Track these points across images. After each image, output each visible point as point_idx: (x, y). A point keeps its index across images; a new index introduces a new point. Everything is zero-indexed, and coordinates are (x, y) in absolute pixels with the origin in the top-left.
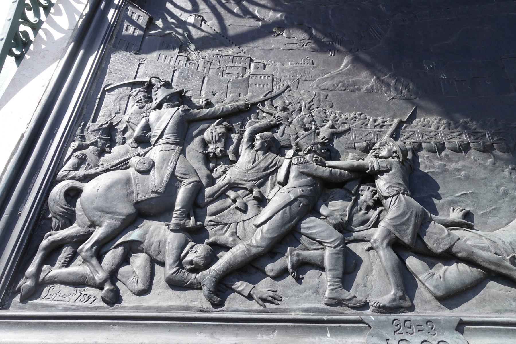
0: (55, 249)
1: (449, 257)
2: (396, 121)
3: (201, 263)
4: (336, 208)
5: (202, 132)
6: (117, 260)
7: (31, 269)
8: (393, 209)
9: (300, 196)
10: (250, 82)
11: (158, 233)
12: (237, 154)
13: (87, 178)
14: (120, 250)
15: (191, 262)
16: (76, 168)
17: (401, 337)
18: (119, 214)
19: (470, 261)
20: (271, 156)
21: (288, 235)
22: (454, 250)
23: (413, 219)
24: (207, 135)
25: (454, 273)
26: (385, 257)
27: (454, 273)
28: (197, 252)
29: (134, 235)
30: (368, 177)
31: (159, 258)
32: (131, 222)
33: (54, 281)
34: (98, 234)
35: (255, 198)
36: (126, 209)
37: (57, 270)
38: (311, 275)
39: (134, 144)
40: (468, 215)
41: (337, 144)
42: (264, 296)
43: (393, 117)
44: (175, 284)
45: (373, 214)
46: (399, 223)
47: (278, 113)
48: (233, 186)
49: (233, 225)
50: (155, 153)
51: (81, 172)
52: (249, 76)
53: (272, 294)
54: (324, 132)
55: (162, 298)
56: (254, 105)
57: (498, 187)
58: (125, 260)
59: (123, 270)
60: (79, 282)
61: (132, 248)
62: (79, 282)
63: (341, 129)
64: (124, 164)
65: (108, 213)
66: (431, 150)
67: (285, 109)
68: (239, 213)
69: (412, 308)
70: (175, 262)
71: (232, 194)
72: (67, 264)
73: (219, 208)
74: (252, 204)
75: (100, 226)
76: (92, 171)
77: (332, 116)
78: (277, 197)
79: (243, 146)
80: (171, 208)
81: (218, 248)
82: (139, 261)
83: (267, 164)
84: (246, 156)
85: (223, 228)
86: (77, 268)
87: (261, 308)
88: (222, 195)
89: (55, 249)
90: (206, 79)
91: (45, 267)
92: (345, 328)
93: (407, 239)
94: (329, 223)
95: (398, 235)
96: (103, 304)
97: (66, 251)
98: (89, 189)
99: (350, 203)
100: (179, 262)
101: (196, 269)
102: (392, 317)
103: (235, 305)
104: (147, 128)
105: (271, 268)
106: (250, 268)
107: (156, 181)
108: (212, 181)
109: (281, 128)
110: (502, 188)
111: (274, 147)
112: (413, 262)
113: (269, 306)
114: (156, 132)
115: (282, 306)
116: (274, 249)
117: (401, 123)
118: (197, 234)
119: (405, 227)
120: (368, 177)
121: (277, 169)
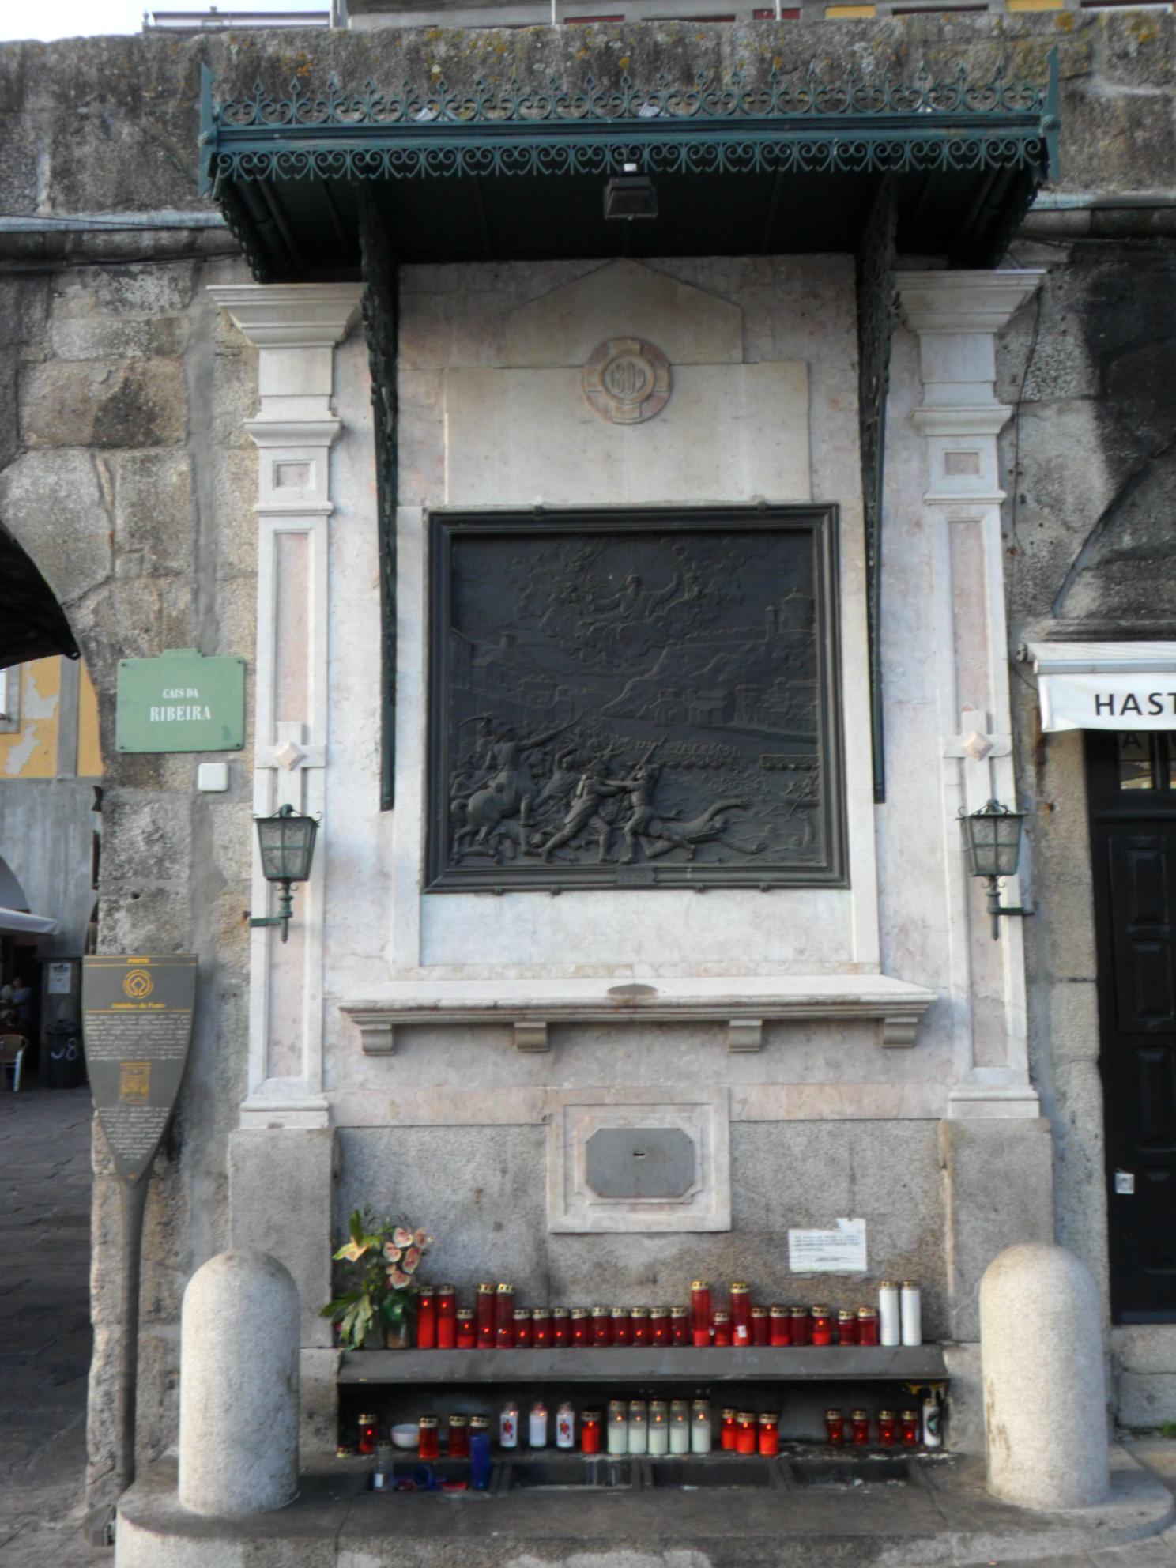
0: (462, 838)
1: (659, 837)
4: (610, 808)
5: (528, 757)
7: (455, 849)
8: (639, 812)
11: (516, 827)
12: (551, 771)
13: (469, 796)
16: (459, 789)
19: (669, 839)
20: (573, 774)
21: (582, 825)
24: (532, 760)
25: (660, 845)
26: (629, 839)
27: (660, 845)
28: (537, 838)
29: (502, 830)
30: (625, 791)
32: (498, 823)
33: (468, 854)
36: (496, 816)
38: (592, 847)
40: (679, 812)
41: (614, 765)
44: (528, 854)
46: (638, 824)
47: (577, 739)
48: (551, 797)
50: (502, 777)
54: (607, 752)
55: (524, 861)
56: (560, 732)
58: (500, 843)
59: (501, 847)
61: (503, 837)
62: (480, 854)
64: (485, 786)
66: (672, 767)
67: (581, 735)
71: (552, 802)
72: (471, 845)
78: (577, 805)
79: (555, 768)
80: (518, 811)
81: (547, 836)
82: (507, 843)
84: (557, 775)
86: (476, 848)
88: (545, 802)
97: (468, 839)
98: (472, 804)
100: (528, 843)
103: (558, 864)
104: (494, 758)
105: (574, 843)
106: (563, 844)
107: (507, 797)
108: (539, 792)
111: (575, 767)
112: (643, 840)
114: (501, 760)
116: (574, 835)
118: (533, 827)
120: (625, 791)
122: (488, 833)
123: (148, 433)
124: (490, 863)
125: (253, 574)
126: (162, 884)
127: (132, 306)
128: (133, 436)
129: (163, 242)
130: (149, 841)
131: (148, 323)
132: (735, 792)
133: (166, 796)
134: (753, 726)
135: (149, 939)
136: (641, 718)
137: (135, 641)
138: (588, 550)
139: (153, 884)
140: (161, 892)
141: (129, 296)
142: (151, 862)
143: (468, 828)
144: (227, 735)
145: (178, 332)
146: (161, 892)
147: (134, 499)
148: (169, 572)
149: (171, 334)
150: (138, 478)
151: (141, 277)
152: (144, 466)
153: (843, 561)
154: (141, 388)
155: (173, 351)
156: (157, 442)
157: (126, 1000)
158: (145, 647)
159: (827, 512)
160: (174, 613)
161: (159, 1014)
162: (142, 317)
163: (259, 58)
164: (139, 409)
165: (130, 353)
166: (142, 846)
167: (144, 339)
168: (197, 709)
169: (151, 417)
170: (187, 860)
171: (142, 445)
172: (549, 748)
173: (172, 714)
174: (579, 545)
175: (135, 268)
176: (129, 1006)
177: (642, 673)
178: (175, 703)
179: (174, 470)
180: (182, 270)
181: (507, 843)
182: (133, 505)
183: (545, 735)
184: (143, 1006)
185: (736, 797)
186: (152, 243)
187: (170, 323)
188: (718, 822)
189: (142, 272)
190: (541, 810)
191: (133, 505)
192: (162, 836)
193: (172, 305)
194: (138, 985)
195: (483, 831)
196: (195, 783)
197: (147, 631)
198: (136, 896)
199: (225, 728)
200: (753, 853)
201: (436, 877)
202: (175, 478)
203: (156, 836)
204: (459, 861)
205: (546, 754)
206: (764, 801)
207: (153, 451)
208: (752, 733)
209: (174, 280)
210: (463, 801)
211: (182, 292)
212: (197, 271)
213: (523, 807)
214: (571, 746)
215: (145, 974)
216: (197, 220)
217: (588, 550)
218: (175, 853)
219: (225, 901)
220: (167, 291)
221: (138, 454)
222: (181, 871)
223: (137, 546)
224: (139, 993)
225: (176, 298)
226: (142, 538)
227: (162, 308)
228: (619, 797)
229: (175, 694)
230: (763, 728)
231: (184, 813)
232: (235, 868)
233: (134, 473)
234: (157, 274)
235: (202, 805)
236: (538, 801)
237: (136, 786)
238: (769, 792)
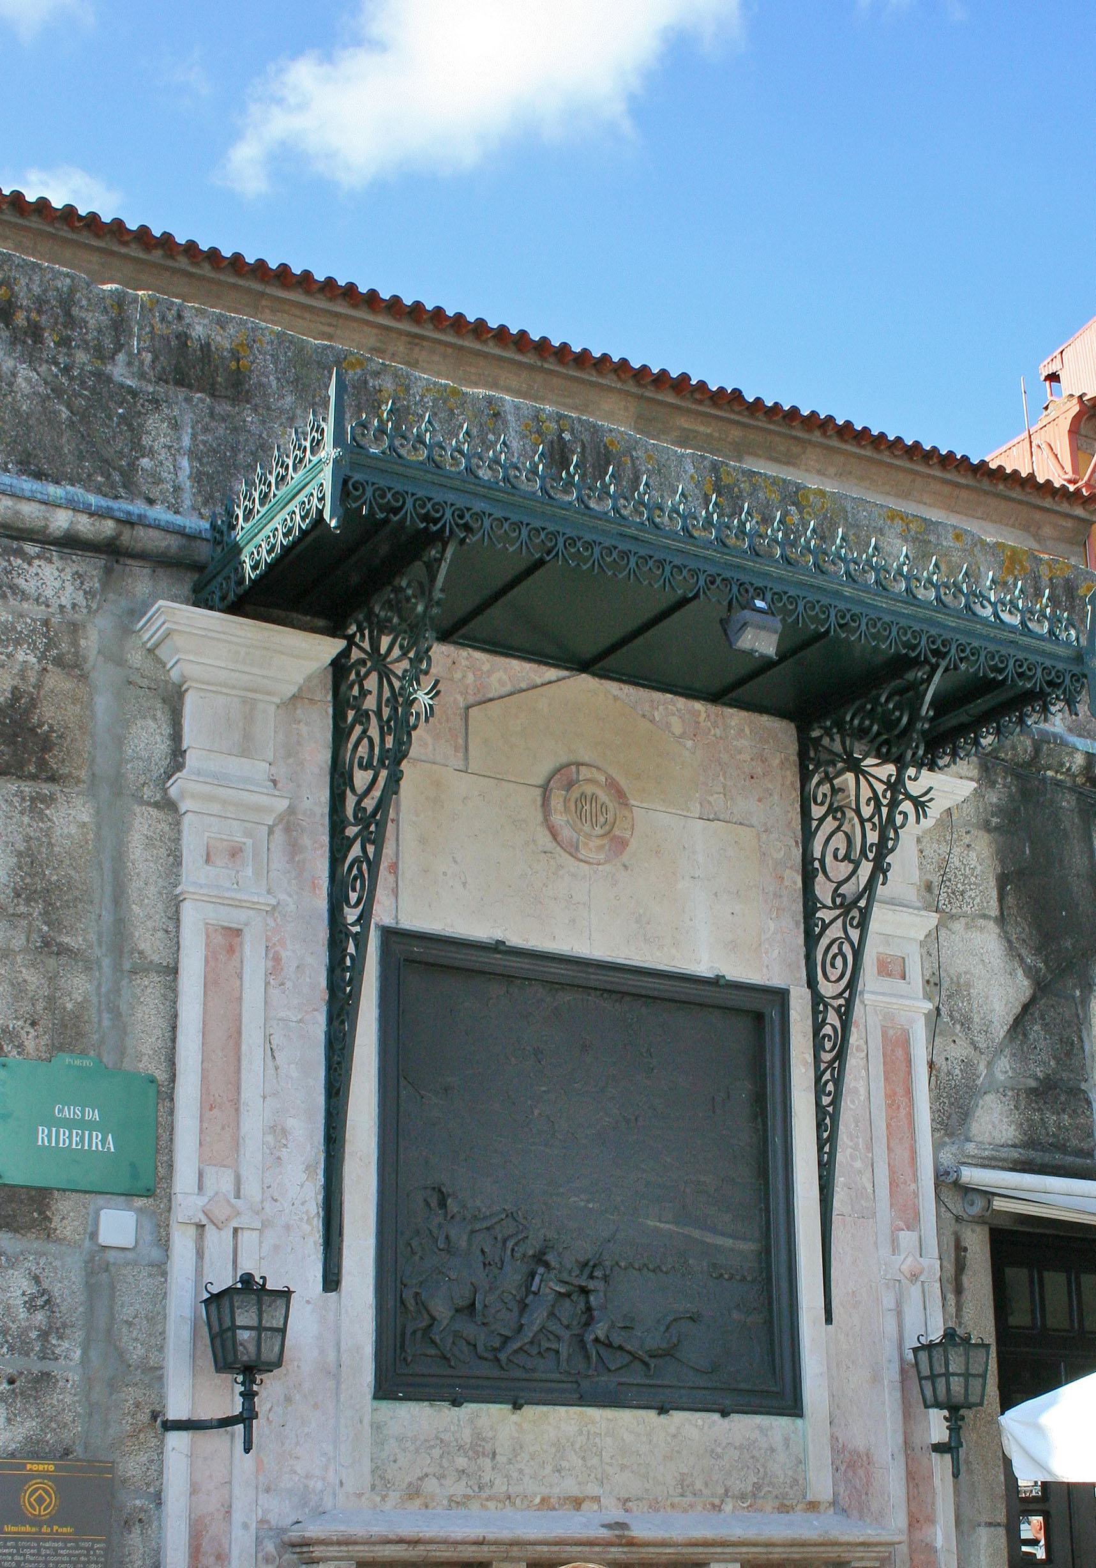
123: (42, 764)
125: (173, 971)
126: (47, 1366)
127: (25, 596)
128: (21, 765)
129: (80, 527)
130: (31, 1306)
131: (46, 623)
133: (52, 1248)
135: (28, 1439)
137: (18, 1036)
139: (37, 1367)
140: (46, 1376)
141: (29, 586)
142: (34, 1334)
144: (135, 1174)
145: (83, 642)
146: (46, 1376)
147: (22, 847)
148: (63, 951)
149: (75, 643)
150: (26, 820)
151: (37, 562)
152: (37, 805)
153: (793, 1054)
154: (33, 703)
155: (76, 666)
156: (52, 779)
157: (20, 1518)
158: (30, 1045)
159: (781, 996)
160: (69, 1006)
161: (65, 1541)
162: (39, 612)
163: (187, 336)
164: (32, 730)
165: (21, 656)
166: (22, 1314)
167: (41, 642)
168: (97, 1137)
169: (46, 745)
170: (79, 1335)
171: (34, 777)
173: (65, 1138)
175: (31, 549)
176: (28, 1528)
178: (70, 1124)
179: (72, 817)
180: (92, 567)
182: (20, 854)
184: (45, 1529)
186: (65, 525)
187: (75, 629)
189: (38, 557)
191: (20, 854)
192: (47, 1302)
193: (74, 605)
194: (40, 1500)
196: (94, 1235)
197: (33, 1024)
198: (11, 1382)
199: (133, 1165)
202: (73, 830)
203: (39, 1302)
207: (46, 788)
209: (77, 575)
211: (89, 594)
212: (108, 571)
215: (49, 1485)
216: (129, 513)
218: (64, 1325)
219: (131, 1394)
220: (69, 588)
221: (27, 788)
222: (70, 1350)
223: (22, 909)
224: (42, 1511)
225: (80, 599)
226: (28, 901)
227: (62, 607)
229: (70, 1112)
231: (76, 1277)
232: (140, 1351)
233: (22, 813)
234: (58, 563)
235: (101, 1268)
237: (16, 1231)
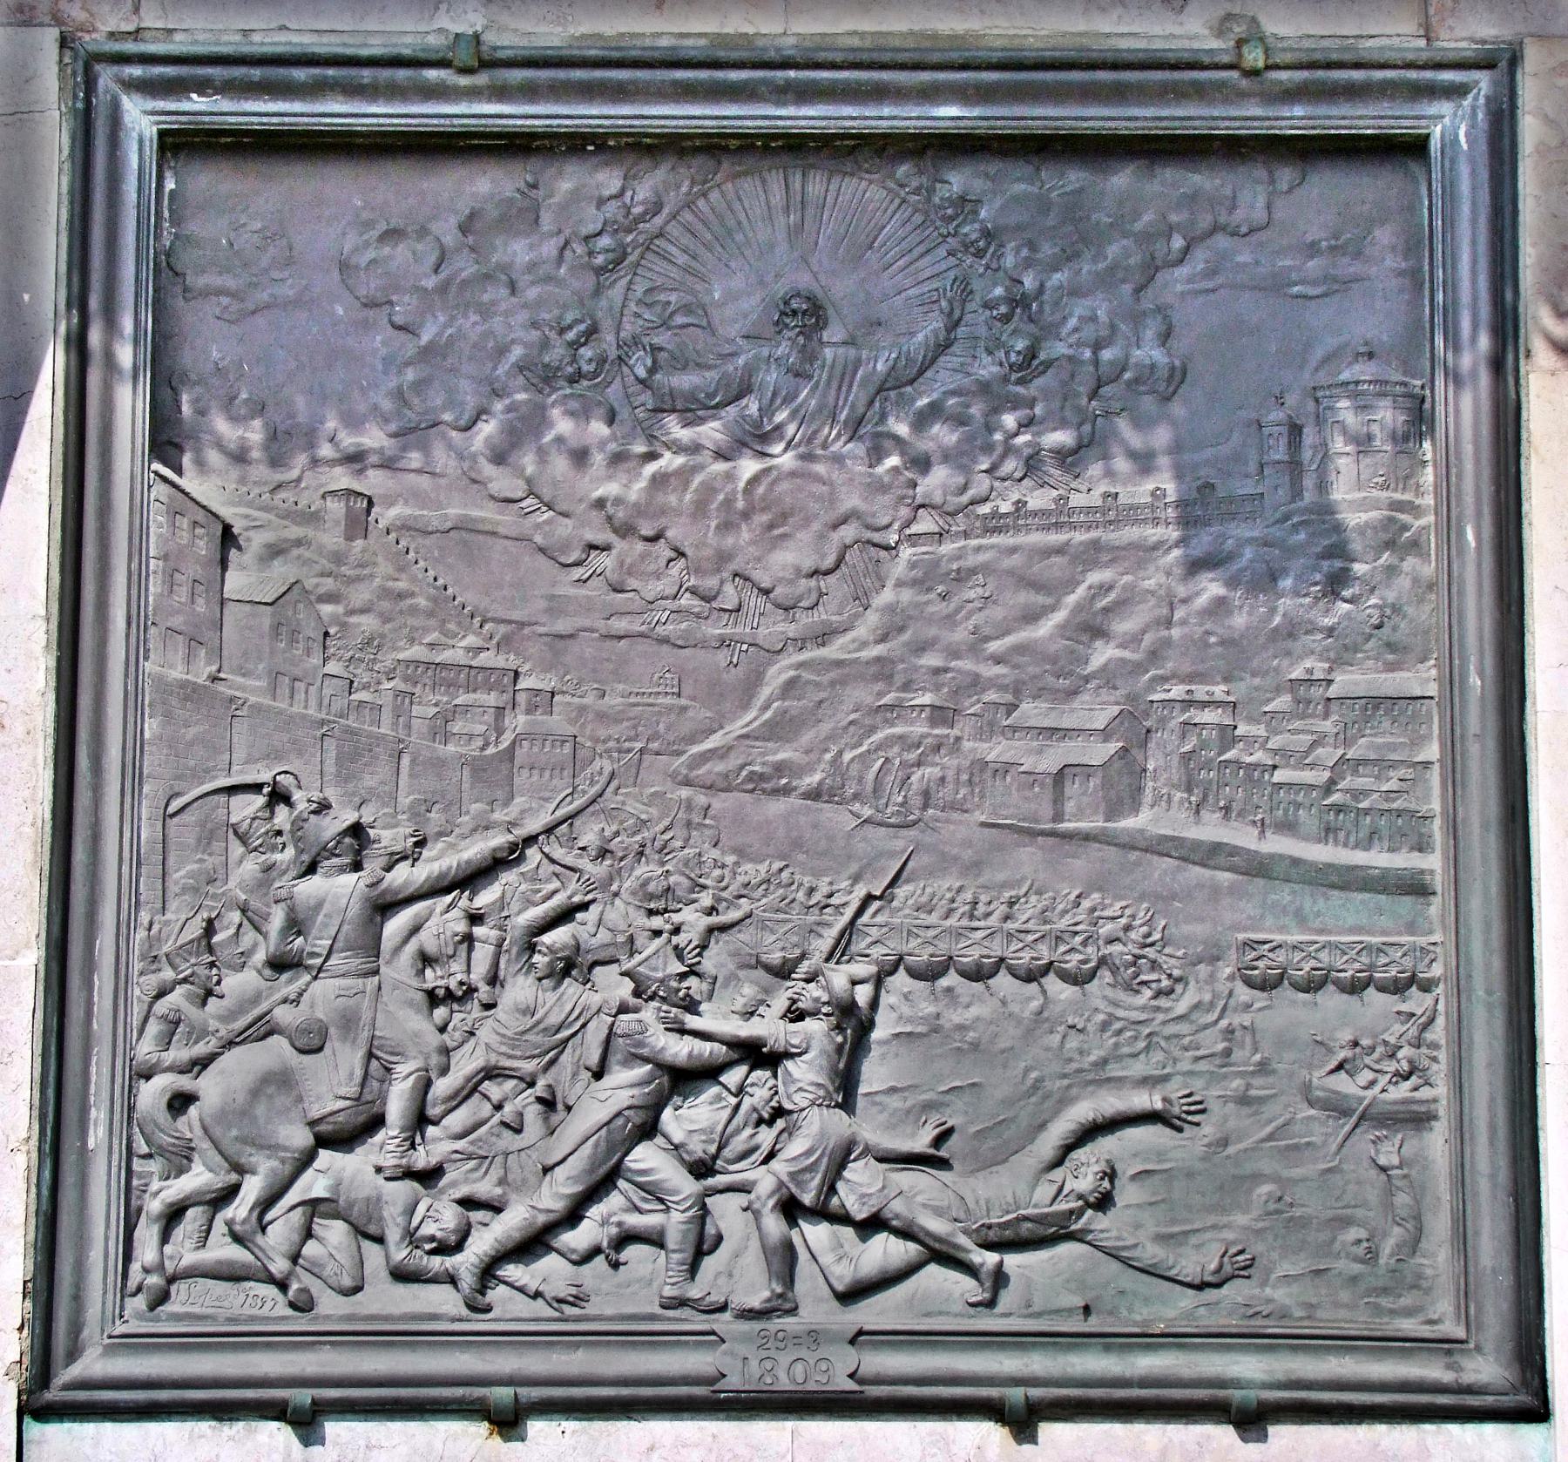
0: (174, 1215)
1: (873, 1225)
2: (860, 892)
3: (453, 1238)
5: (415, 930)
6: (296, 1238)
9: (629, 1108)
10: (517, 762)
14: (297, 1216)
15: (432, 1239)
17: (765, 1354)
18: (285, 1149)
19: (906, 1234)
22: (887, 1214)
23: (825, 1160)
29: (313, 1184)
31: (372, 1229)
34: (252, 1189)
35: (540, 1100)
37: (184, 1250)
39: (268, 972)
40: (941, 1139)
42: (562, 1295)
43: (856, 879)
44: (402, 1275)
45: (766, 1136)
48: (491, 1073)
49: (499, 1159)
51: (179, 1053)
52: (514, 742)
53: (574, 1291)
56: (531, 840)
57: (1027, 1070)
60: (232, 1275)
62: (232, 1275)
63: (733, 915)
65: (262, 1147)
68: (507, 1134)
69: (793, 1311)
70: (403, 1238)
71: (494, 1090)
73: (469, 1122)
74: (533, 1113)
75: (253, 1172)
76: (201, 1049)
77: (717, 872)
83: (563, 1016)
85: (480, 1165)
86: (221, 1250)
87: (557, 1314)
89: (174, 1215)
90: (406, 761)
91: (168, 1249)
92: (686, 1343)
93: (807, 1199)
94: (682, 1161)
95: (794, 1190)
96: (290, 1312)
99: (726, 1114)
101: (444, 1249)
102: (756, 1326)
109: (594, 910)
110: (1034, 1075)
113: (570, 1311)
115: (590, 1309)
117: (869, 898)
119: (808, 1176)
121: (584, 1026)
122: (267, 1203)
124: (265, 1302)
132: (1138, 1068)
134: (1211, 829)
136: (814, 795)
138: (643, 191)
143: (199, 1177)
172: (486, 897)
174: (609, 179)
177: (824, 636)
181: (334, 1232)
183: (475, 850)
185: (1147, 1082)
188: (1083, 1176)
190: (457, 1120)
195: (252, 1189)
200: (1201, 1287)
201: (73, 1355)
204: (162, 1297)
205: (475, 919)
206: (1244, 1100)
208: (1212, 854)
210: (185, 1083)
213: (396, 1107)
214: (571, 892)
217: (643, 191)
228: (733, 1077)
230: (1243, 837)
236: (442, 1086)
238: (1263, 1068)
